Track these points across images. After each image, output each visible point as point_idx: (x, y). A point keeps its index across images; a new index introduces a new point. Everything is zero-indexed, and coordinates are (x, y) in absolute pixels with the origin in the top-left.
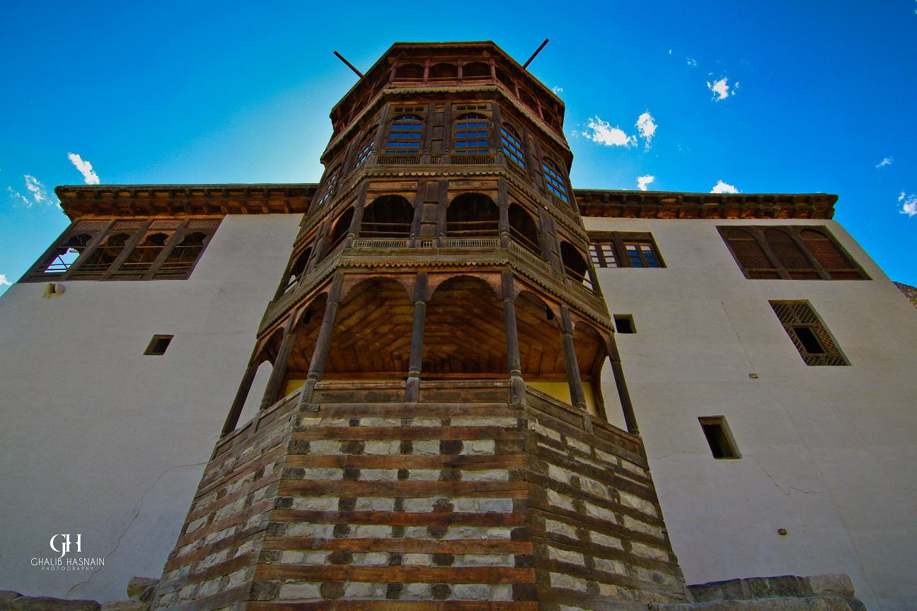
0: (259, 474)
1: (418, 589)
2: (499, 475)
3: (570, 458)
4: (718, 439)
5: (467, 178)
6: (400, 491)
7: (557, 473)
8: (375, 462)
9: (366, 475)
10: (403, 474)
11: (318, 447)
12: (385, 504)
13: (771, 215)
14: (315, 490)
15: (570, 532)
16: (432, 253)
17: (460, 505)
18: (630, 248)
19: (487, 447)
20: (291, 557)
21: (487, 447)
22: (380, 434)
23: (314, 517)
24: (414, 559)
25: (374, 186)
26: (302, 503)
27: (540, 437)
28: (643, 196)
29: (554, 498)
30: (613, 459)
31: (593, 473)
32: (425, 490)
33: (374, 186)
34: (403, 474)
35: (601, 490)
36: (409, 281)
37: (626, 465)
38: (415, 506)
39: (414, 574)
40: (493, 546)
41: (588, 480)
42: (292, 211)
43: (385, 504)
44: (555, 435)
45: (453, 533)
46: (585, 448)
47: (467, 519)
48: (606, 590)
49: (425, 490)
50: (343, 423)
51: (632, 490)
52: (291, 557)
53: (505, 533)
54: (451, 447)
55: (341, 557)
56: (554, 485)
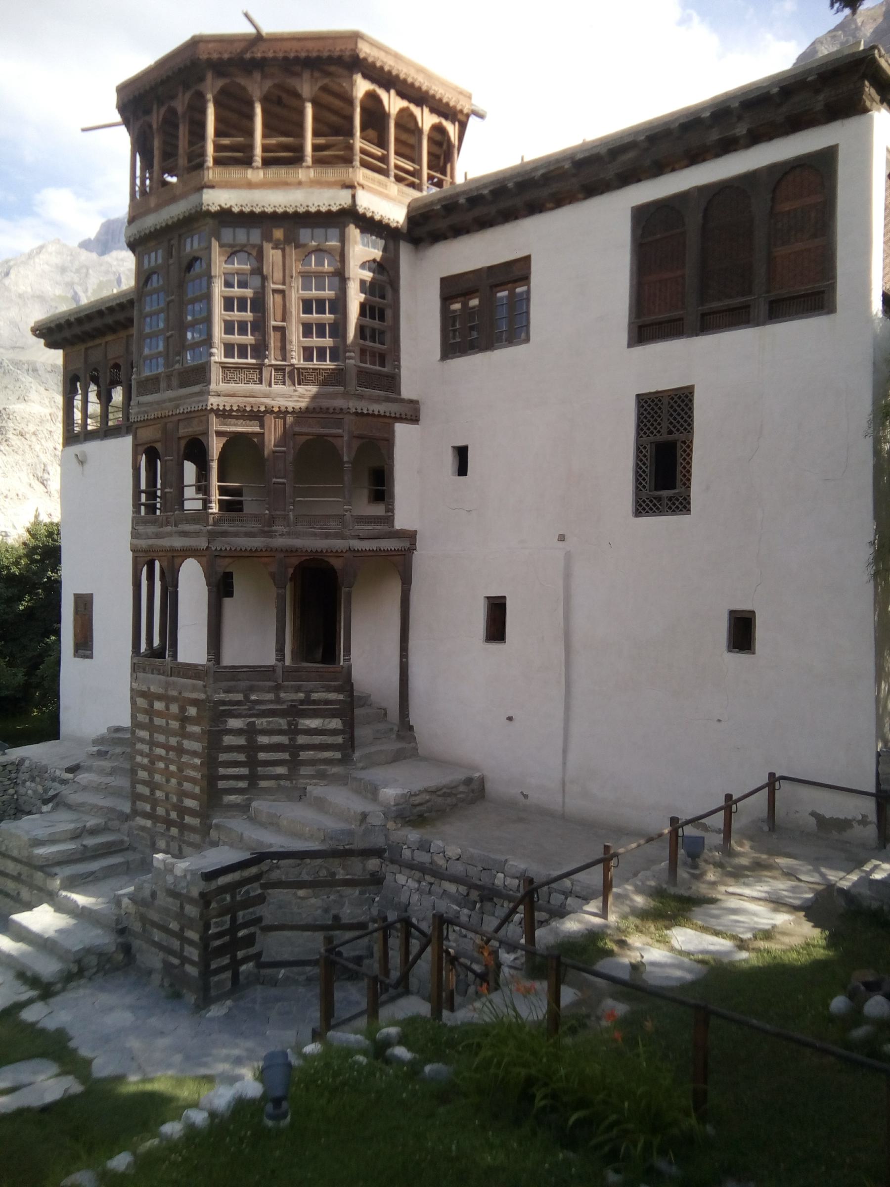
3: (250, 709)
7: (234, 723)
10: (167, 724)
15: (242, 757)
16: (170, 535)
23: (142, 741)
24: (173, 768)
27: (224, 703)
28: (510, 185)
29: (228, 740)
30: (301, 695)
31: (272, 713)
32: (174, 734)
34: (167, 724)
35: (283, 723)
37: (315, 696)
38: (173, 741)
40: (194, 767)
41: (264, 720)
44: (239, 697)
46: (270, 696)
47: (187, 752)
48: (263, 784)
51: (315, 714)
53: (198, 761)
54: (183, 709)
56: (231, 732)
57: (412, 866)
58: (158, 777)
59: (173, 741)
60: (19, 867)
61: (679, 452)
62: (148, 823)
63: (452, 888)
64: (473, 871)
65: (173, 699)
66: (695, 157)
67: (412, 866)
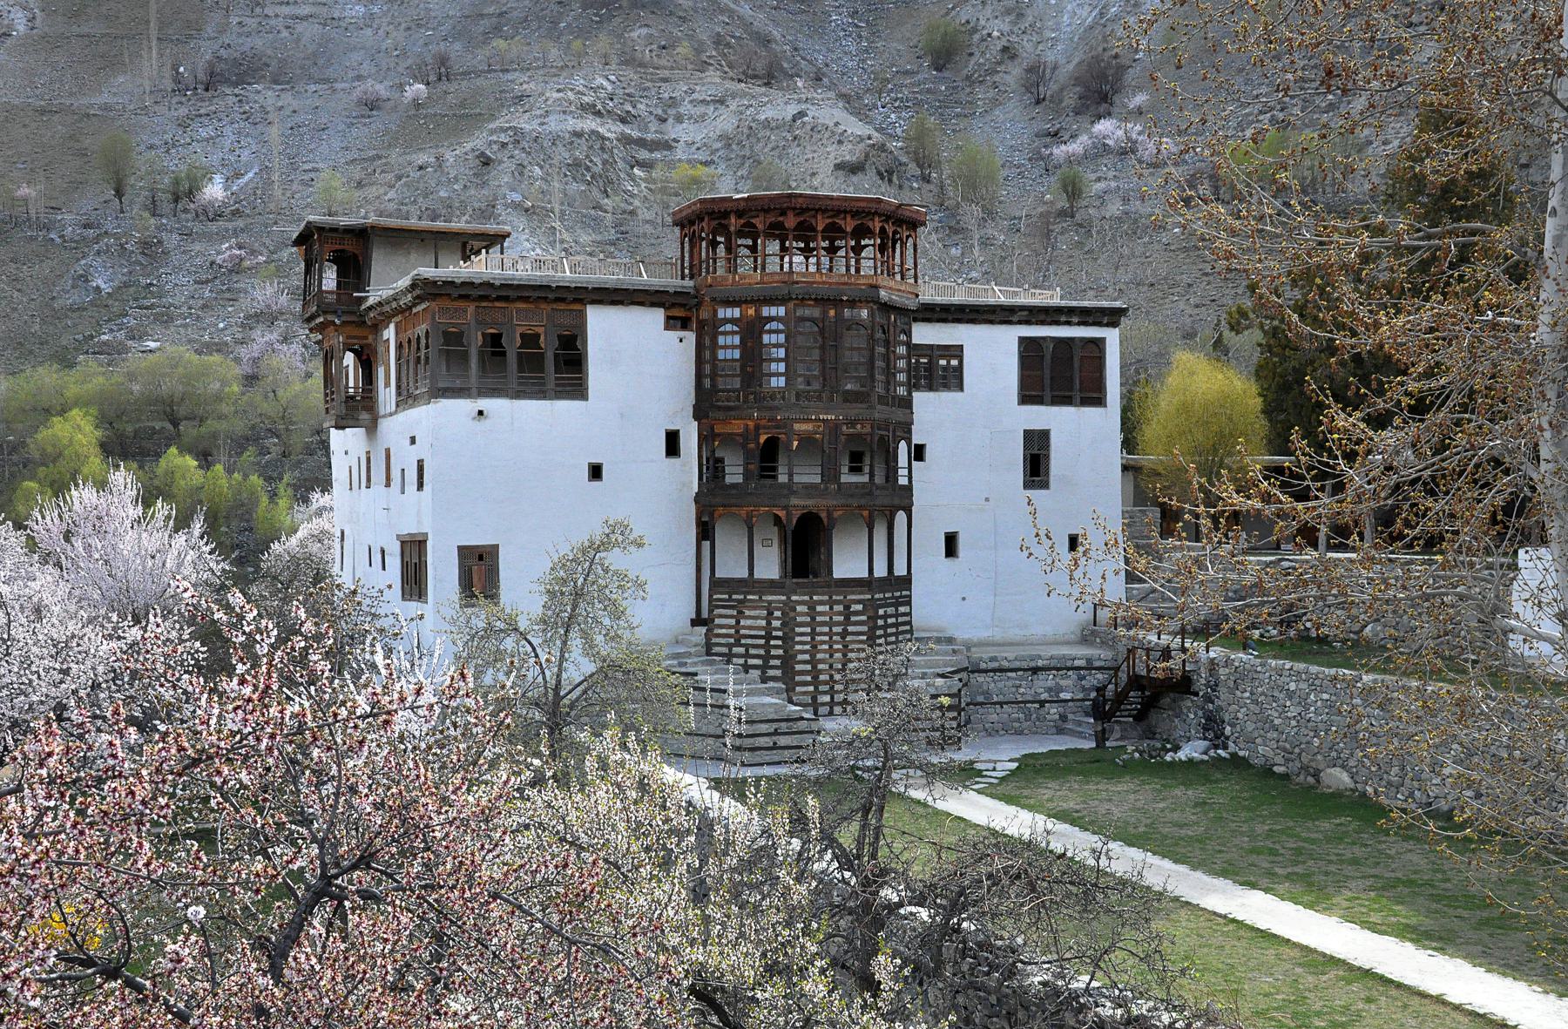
0: (770, 614)
1: (838, 655)
2: (864, 618)
4: (951, 545)
5: (852, 423)
6: (831, 624)
7: (881, 612)
8: (822, 614)
9: (819, 619)
11: (799, 608)
12: (826, 629)
13: (1068, 323)
14: (802, 625)
17: (850, 629)
18: (943, 362)
19: (860, 607)
20: (798, 647)
21: (860, 607)
22: (821, 603)
25: (797, 427)
26: (798, 630)
32: (838, 624)
33: (797, 427)
35: (891, 610)
36: (823, 515)
38: (835, 629)
39: (838, 651)
42: (653, 305)
43: (826, 629)
45: (849, 638)
49: (838, 624)
50: (806, 598)
51: (902, 604)
52: (798, 647)
54: (847, 607)
55: (814, 647)
57: (986, 671)
58: (819, 656)
59: (835, 629)
60: (775, 725)
61: (1042, 460)
62: (811, 688)
63: (1013, 675)
64: (1024, 665)
65: (838, 602)
66: (1042, 323)
67: (986, 671)
